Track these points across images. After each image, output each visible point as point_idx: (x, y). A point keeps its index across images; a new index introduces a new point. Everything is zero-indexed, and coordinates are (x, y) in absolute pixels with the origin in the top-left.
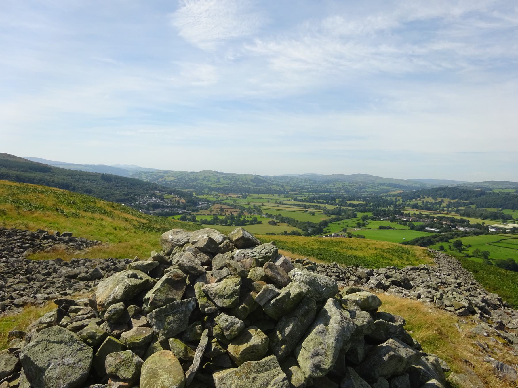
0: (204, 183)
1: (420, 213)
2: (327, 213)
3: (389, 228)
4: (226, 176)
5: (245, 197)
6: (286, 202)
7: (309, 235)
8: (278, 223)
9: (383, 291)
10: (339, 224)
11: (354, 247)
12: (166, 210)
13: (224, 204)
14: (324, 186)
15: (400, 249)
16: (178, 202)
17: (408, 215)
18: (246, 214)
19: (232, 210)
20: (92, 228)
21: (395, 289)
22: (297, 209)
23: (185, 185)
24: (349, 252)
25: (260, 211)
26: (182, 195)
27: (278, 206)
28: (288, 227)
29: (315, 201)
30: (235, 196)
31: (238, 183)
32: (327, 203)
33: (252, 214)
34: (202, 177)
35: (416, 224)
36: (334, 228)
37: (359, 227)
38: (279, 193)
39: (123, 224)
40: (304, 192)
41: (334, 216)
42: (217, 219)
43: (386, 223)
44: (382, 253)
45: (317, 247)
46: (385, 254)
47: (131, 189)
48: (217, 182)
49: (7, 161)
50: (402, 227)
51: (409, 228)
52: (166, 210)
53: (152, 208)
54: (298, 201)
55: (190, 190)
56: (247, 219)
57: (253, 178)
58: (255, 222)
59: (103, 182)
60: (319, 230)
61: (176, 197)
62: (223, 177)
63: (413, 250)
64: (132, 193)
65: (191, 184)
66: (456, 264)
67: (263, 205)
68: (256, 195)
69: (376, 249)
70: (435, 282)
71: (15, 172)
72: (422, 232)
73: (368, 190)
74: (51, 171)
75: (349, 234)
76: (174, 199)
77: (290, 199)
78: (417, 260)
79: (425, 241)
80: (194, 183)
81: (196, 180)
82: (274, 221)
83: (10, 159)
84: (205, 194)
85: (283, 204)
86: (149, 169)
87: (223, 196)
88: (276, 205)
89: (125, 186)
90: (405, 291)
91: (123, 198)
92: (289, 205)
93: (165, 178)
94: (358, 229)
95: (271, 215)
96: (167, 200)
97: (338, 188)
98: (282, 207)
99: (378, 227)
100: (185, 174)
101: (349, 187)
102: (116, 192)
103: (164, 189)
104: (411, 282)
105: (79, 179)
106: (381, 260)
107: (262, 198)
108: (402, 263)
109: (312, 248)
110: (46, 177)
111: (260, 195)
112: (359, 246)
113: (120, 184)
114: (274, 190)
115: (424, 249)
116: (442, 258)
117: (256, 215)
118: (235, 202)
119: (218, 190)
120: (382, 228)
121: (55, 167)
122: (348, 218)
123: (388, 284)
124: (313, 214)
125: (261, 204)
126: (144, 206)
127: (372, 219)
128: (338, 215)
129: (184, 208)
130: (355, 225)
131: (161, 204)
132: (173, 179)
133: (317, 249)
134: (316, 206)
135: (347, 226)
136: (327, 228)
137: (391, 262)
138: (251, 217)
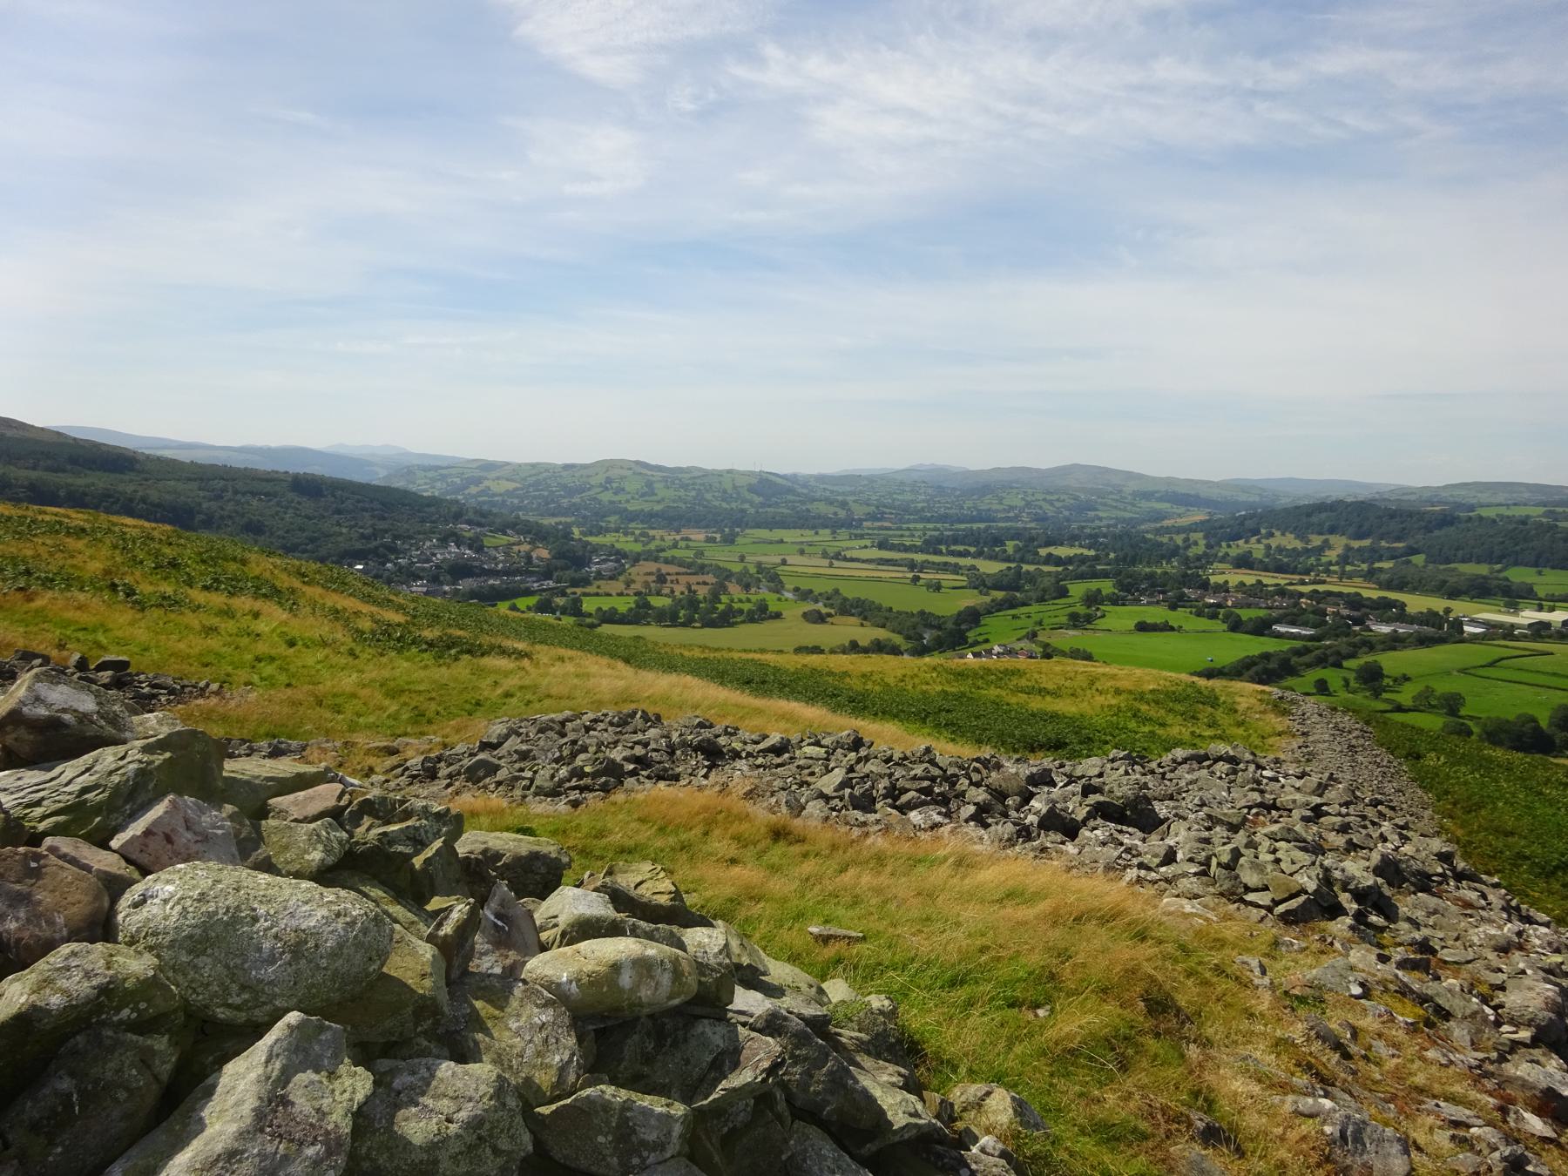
0: (606, 497)
1: (1259, 582)
2: (980, 583)
3: (1166, 628)
5: (730, 540)
7: (921, 651)
8: (830, 615)
9: (1059, 837)
10: (1014, 617)
11: (1050, 686)
13: (667, 561)
14: (969, 504)
15: (1189, 690)
16: (529, 558)
17: (1223, 588)
18: (735, 590)
19: (693, 579)
20: (214, 643)
21: (1102, 830)
22: (887, 573)
24: (1036, 704)
25: (775, 581)
26: (538, 535)
27: (831, 565)
28: (861, 630)
29: (943, 548)
30: (702, 537)
31: (708, 496)
32: (979, 555)
33: (753, 590)
34: (601, 479)
35: (1245, 614)
36: (1001, 630)
37: (1075, 627)
38: (834, 525)
39: (322, 628)
40: (909, 521)
41: (999, 595)
42: (647, 605)
43: (1156, 614)
44: (1137, 704)
45: (939, 688)
46: (1144, 707)
47: (384, 519)
48: (643, 495)
50: (1204, 623)
51: (1225, 626)
52: (491, 582)
54: (892, 548)
55: (563, 519)
56: (736, 606)
58: (761, 614)
60: (955, 634)
61: (519, 543)
62: (665, 479)
63: (1228, 694)
64: (386, 531)
65: (565, 502)
66: (1356, 733)
67: (784, 562)
68: (764, 533)
69: (1118, 692)
70: (1243, 803)
71: (23, 473)
72: (1262, 639)
73: (1101, 514)
74: (138, 466)
75: (1047, 645)
76: (516, 548)
77: (868, 543)
78: (1239, 724)
79: (1271, 666)
80: (576, 500)
82: (819, 612)
83: (9, 433)
84: (608, 530)
85: (845, 559)
87: (662, 536)
88: (826, 562)
90: (1132, 837)
91: (358, 546)
92: (864, 561)
93: (486, 483)
94: (1071, 632)
95: (811, 591)
96: (493, 553)
97: (1012, 508)
98: (841, 568)
99: (1131, 624)
101: (1046, 506)
102: (337, 529)
103: (485, 518)
104: (1157, 806)
105: (224, 490)
106: (1132, 725)
107: (782, 541)
108: (1193, 733)
109: (924, 692)
110: (121, 488)
111: (778, 534)
112: (1068, 683)
113: (348, 504)
115: (1263, 692)
116: (1315, 718)
117: (765, 594)
118: (700, 554)
119: (649, 518)
120: (1142, 627)
121: (148, 457)
122: (1041, 600)
123: (1081, 814)
124: (938, 587)
125: (778, 560)
126: (424, 569)
127: (1115, 601)
128: (1013, 592)
129: (547, 575)
130: (1064, 619)
132: (511, 486)
133: (939, 693)
134: (946, 564)
135: (1040, 623)
136: (979, 630)
137: (1160, 731)
138: (749, 600)
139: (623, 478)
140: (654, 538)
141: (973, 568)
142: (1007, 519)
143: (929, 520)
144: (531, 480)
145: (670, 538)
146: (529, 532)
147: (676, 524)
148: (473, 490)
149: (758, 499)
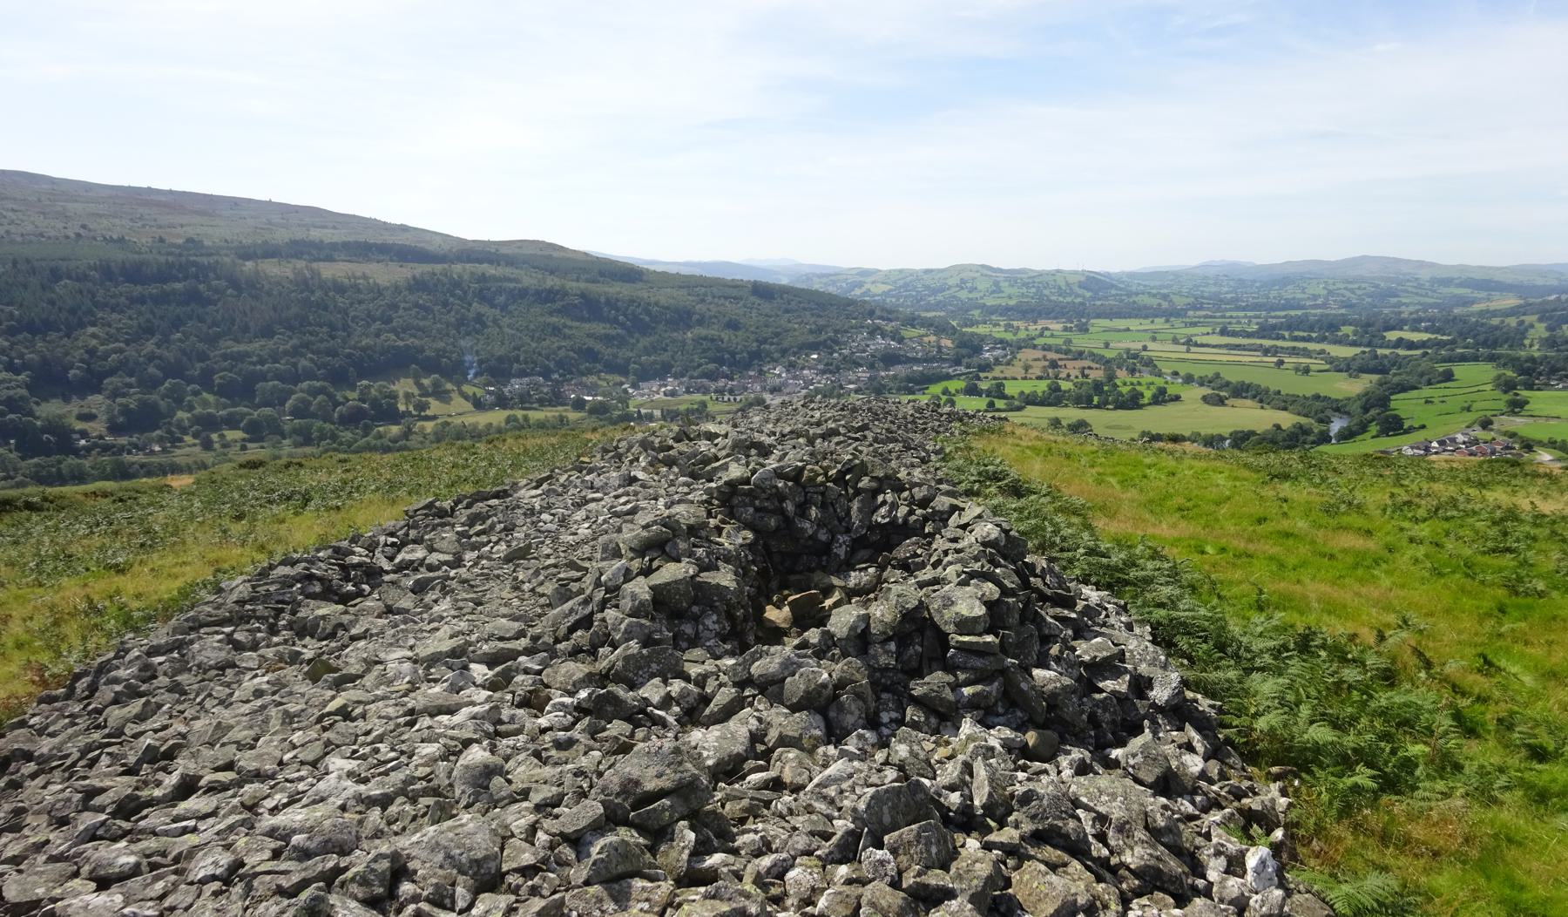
5: (1083, 329)
6: (1205, 340)
14: (1273, 294)
16: (940, 348)
22: (1246, 358)
26: (941, 328)
29: (1287, 334)
30: (1059, 326)
38: (1170, 314)
40: (1227, 310)
49: (550, 257)
68: (1105, 323)
71: (574, 284)
77: (1209, 330)
83: (555, 254)
86: (824, 267)
91: (811, 339)
107: (1128, 330)
110: (639, 293)
124: (1307, 371)
129: (957, 362)
143: (1244, 309)
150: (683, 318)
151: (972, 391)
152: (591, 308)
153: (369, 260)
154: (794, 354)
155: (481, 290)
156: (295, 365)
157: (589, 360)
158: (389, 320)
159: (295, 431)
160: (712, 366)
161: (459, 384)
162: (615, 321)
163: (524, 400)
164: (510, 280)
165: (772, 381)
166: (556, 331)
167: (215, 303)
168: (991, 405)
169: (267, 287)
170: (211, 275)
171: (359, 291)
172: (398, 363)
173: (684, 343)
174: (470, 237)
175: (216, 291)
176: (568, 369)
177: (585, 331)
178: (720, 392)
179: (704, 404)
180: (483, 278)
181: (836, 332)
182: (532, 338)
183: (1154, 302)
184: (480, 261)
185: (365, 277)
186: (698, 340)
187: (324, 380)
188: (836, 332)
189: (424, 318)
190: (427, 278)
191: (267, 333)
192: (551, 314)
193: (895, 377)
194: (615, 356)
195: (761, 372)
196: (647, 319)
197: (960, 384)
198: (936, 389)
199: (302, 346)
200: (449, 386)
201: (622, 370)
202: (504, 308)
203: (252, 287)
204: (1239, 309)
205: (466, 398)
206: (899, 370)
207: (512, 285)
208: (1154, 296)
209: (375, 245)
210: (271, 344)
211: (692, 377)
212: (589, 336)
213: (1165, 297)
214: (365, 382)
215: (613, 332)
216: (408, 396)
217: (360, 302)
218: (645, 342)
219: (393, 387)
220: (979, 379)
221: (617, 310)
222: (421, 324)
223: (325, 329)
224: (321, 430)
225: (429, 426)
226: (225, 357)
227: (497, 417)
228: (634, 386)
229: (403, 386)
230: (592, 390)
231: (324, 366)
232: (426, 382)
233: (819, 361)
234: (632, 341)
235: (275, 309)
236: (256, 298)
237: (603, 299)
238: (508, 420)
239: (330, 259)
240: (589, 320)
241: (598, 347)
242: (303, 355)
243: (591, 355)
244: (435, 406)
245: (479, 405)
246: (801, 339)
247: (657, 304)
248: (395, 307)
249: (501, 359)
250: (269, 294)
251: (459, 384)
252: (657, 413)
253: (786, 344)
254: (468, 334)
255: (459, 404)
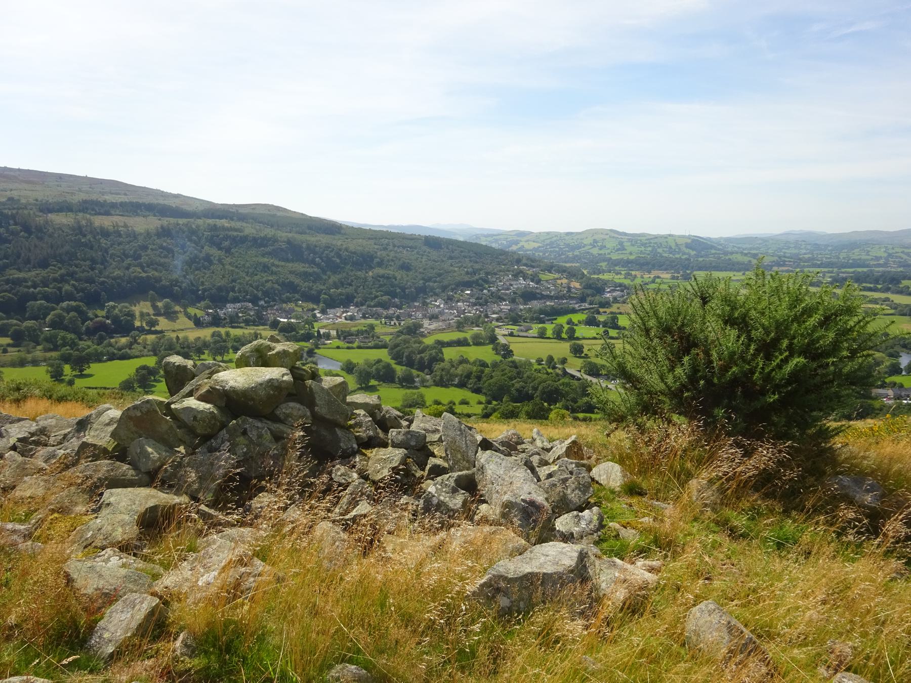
0: (595, 251)
4: (634, 239)
12: (548, 303)
16: (569, 288)
23: (560, 255)
26: (572, 274)
30: (669, 276)
31: (660, 250)
32: (887, 290)
47: (477, 262)
48: (618, 250)
49: (274, 216)
52: (548, 303)
53: (521, 300)
57: (689, 241)
59: (428, 250)
62: (629, 240)
64: (481, 270)
65: (570, 254)
71: (284, 234)
74: (343, 231)
76: (559, 282)
80: (577, 253)
81: (579, 247)
83: (279, 214)
84: (603, 272)
87: (641, 277)
89: (465, 257)
91: (467, 278)
97: (878, 258)
100: (556, 236)
101: (905, 257)
105: (388, 245)
110: (334, 242)
114: (738, 263)
119: (627, 263)
126: (506, 294)
129: (583, 300)
131: (538, 291)
132: (536, 245)
139: (604, 240)
140: (635, 276)
141: (887, 299)
142: (879, 265)
143: (819, 266)
144: (548, 242)
145: (647, 277)
146: (564, 271)
147: (645, 267)
148: (514, 248)
149: (693, 253)
150: (366, 261)
151: (591, 322)
152: (295, 252)
153: (138, 215)
154: (452, 290)
155: (212, 236)
156: (60, 289)
157: (290, 291)
158: (137, 257)
159: (48, 340)
160: (385, 298)
161: (185, 307)
162: (313, 262)
163: (233, 321)
164: (236, 230)
165: (432, 310)
166: (266, 268)
167: (9, 242)
168: (606, 332)
169: (51, 230)
170: (11, 222)
171: (120, 235)
172: (140, 289)
173: (365, 279)
174: (216, 201)
175: (13, 233)
176: (272, 297)
177: (289, 270)
178: (389, 318)
179: (372, 327)
180: (214, 228)
181: (487, 274)
182: (247, 273)
183: (746, 259)
184: (220, 217)
185: (126, 226)
186: (377, 278)
187: (81, 301)
188: (487, 274)
189: (166, 257)
190: (171, 227)
191: (44, 264)
192: (263, 255)
193: (530, 310)
194: (310, 289)
195: (425, 304)
196: (338, 261)
197: (582, 317)
198: (562, 320)
199: (68, 274)
200: (177, 308)
201: (315, 299)
202: (228, 250)
203: (40, 231)
204: (815, 266)
205: (189, 318)
206: (536, 305)
207: (235, 234)
208: (746, 255)
209: (144, 204)
210: (43, 273)
211: (368, 306)
212: (291, 272)
213: (755, 256)
214: (111, 303)
215: (310, 270)
216: (142, 315)
217: (119, 244)
218: (334, 278)
219: (133, 308)
220: (599, 313)
221: (315, 253)
222: (162, 260)
223: (88, 263)
224: (63, 338)
225: (151, 338)
226: (7, 282)
227: (206, 334)
228: (323, 312)
229: (142, 308)
230: (288, 313)
231: (82, 290)
232: (160, 304)
233: (471, 295)
234: (325, 277)
235: (52, 247)
236: (41, 239)
237: (304, 245)
238: (213, 335)
239: (107, 214)
240: (292, 261)
241: (297, 281)
242: (67, 282)
243: (292, 288)
244: (163, 323)
245: (198, 323)
246: (458, 279)
247: (346, 249)
248: (145, 248)
249: (220, 289)
250: (51, 236)
251: (185, 307)
252: (333, 333)
253: (446, 283)
254: (197, 269)
255: (183, 321)
